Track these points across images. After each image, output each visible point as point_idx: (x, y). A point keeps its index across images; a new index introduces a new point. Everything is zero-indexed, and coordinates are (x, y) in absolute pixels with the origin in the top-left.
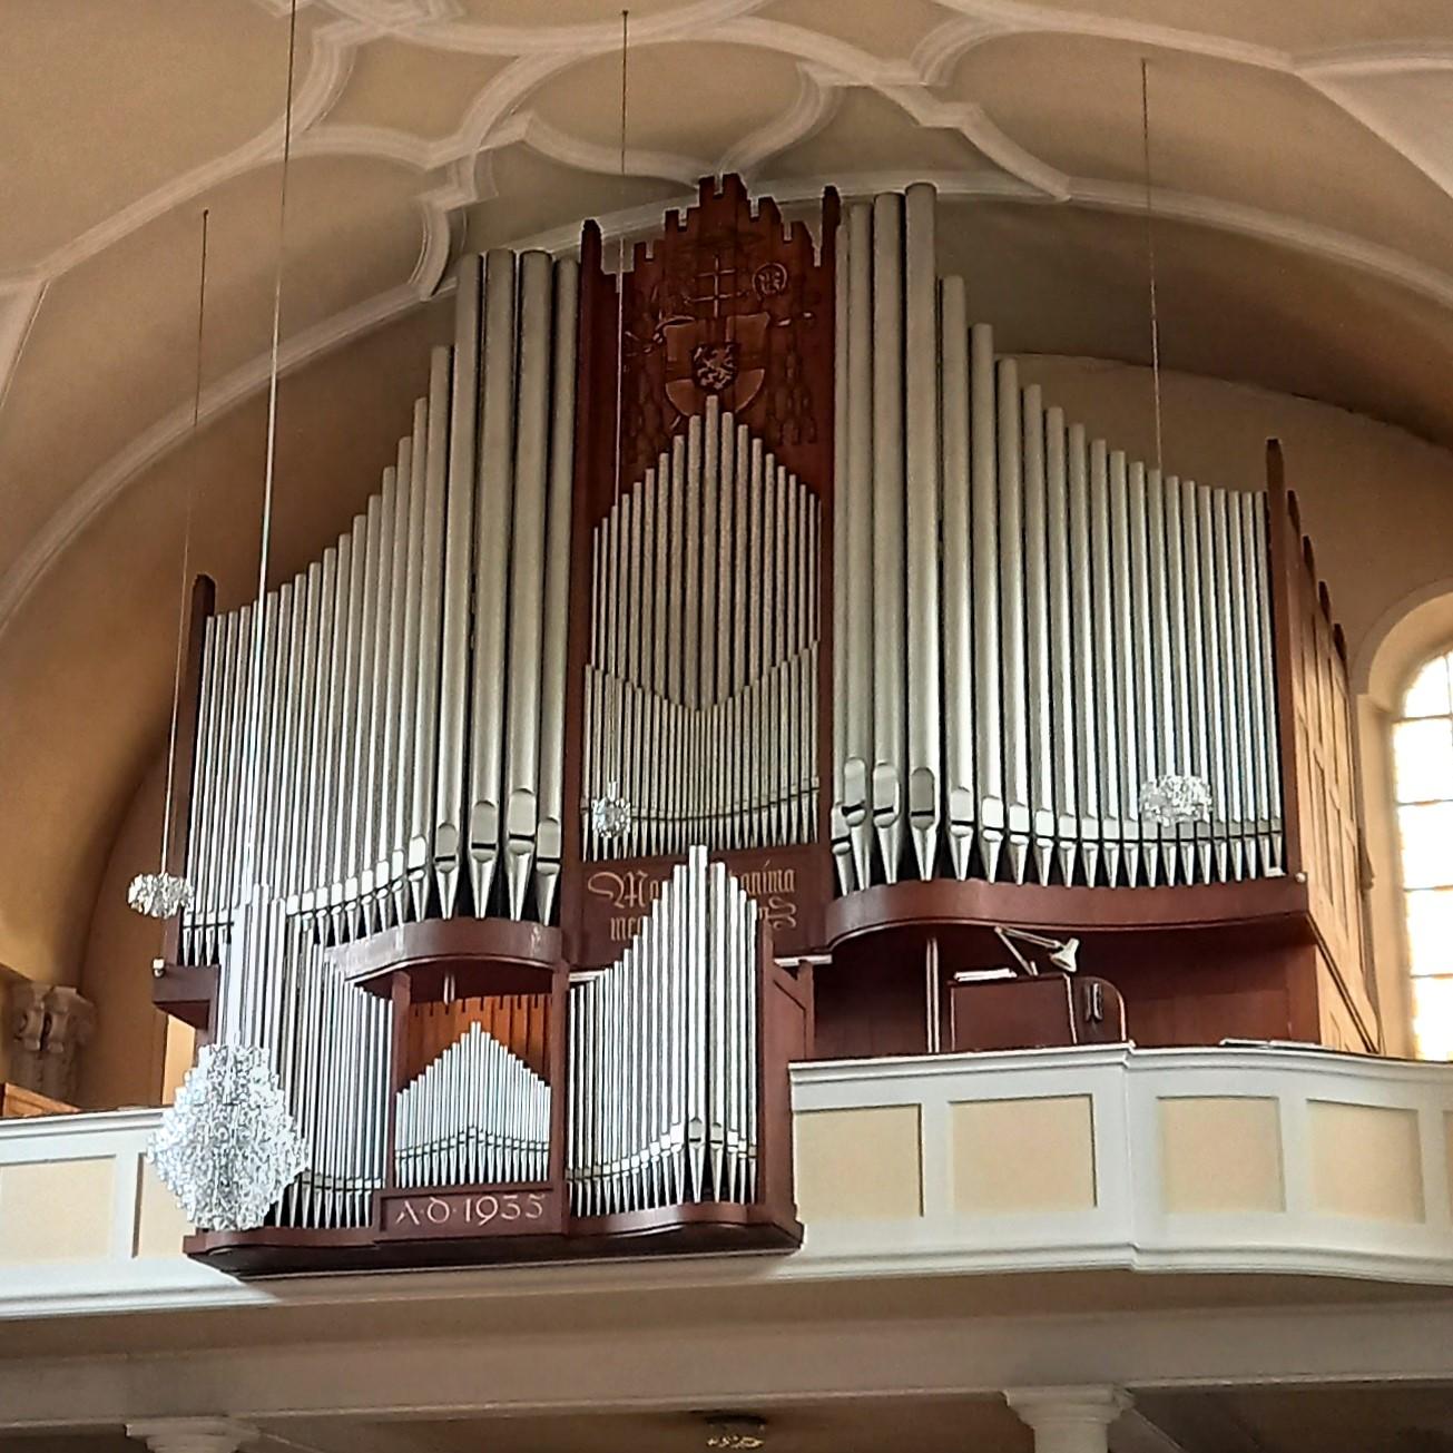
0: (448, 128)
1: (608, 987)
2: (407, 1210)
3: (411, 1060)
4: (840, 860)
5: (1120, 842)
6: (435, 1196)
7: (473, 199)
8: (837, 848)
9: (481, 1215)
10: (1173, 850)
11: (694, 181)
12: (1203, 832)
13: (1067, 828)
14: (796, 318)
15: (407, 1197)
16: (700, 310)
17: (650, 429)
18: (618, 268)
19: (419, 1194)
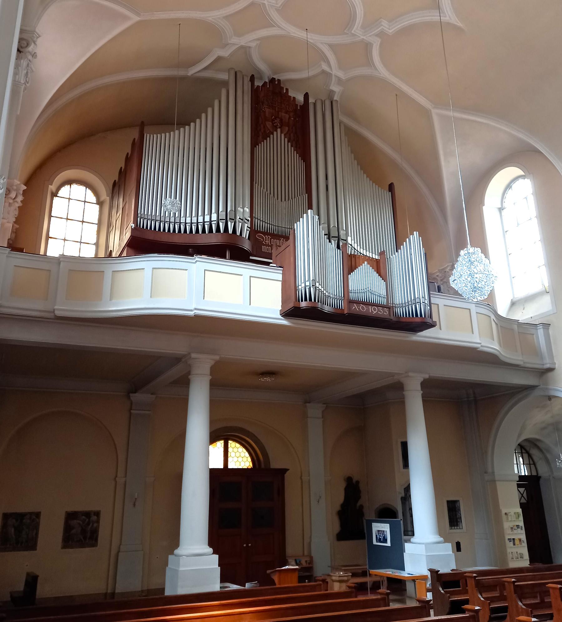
2: (355, 306)
6: (362, 304)
9: (373, 311)
15: (355, 303)
17: (262, 130)
19: (358, 302)
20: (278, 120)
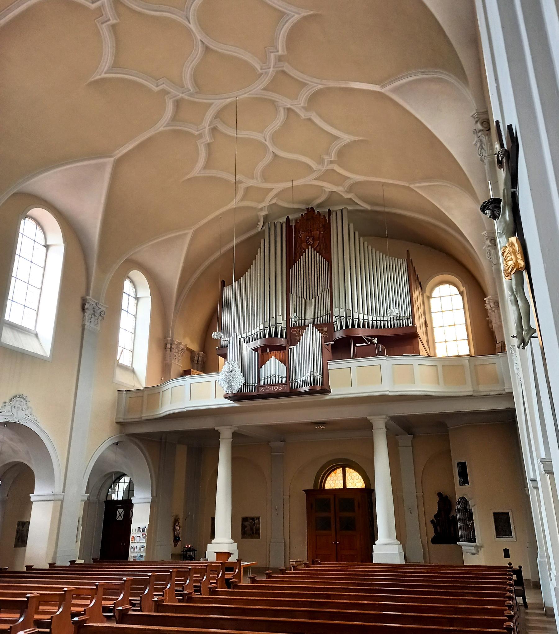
0: (263, 201)
1: (296, 349)
3: (262, 363)
4: (335, 325)
5: (384, 320)
6: (267, 386)
7: (267, 213)
8: (334, 323)
9: (275, 389)
10: (393, 322)
11: (305, 208)
12: (398, 318)
13: (374, 318)
14: (324, 232)
15: (262, 386)
16: (307, 231)
18: (293, 224)
19: (264, 386)
20: (311, 238)
